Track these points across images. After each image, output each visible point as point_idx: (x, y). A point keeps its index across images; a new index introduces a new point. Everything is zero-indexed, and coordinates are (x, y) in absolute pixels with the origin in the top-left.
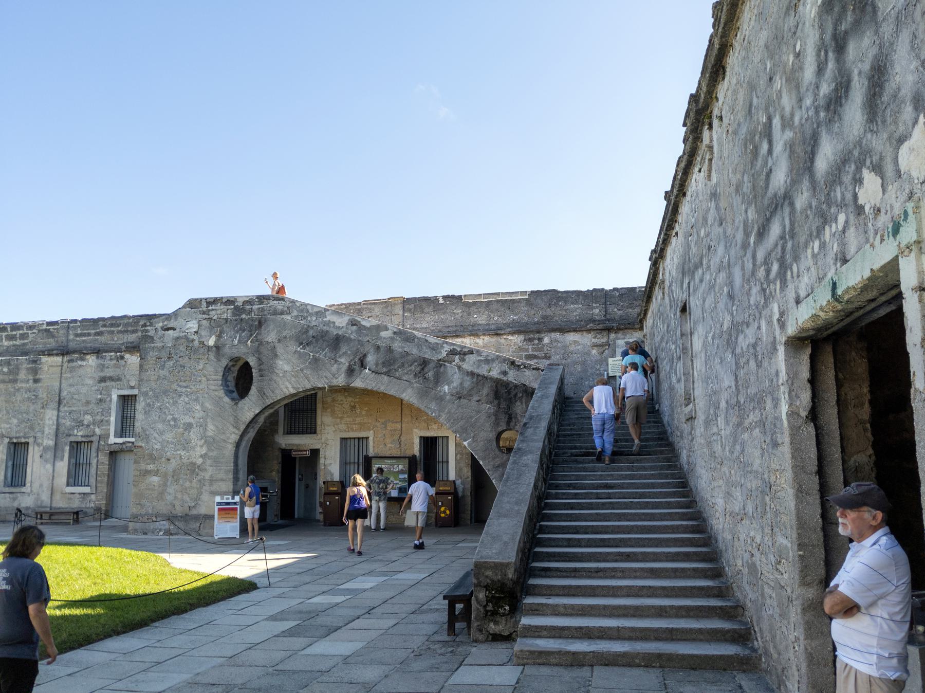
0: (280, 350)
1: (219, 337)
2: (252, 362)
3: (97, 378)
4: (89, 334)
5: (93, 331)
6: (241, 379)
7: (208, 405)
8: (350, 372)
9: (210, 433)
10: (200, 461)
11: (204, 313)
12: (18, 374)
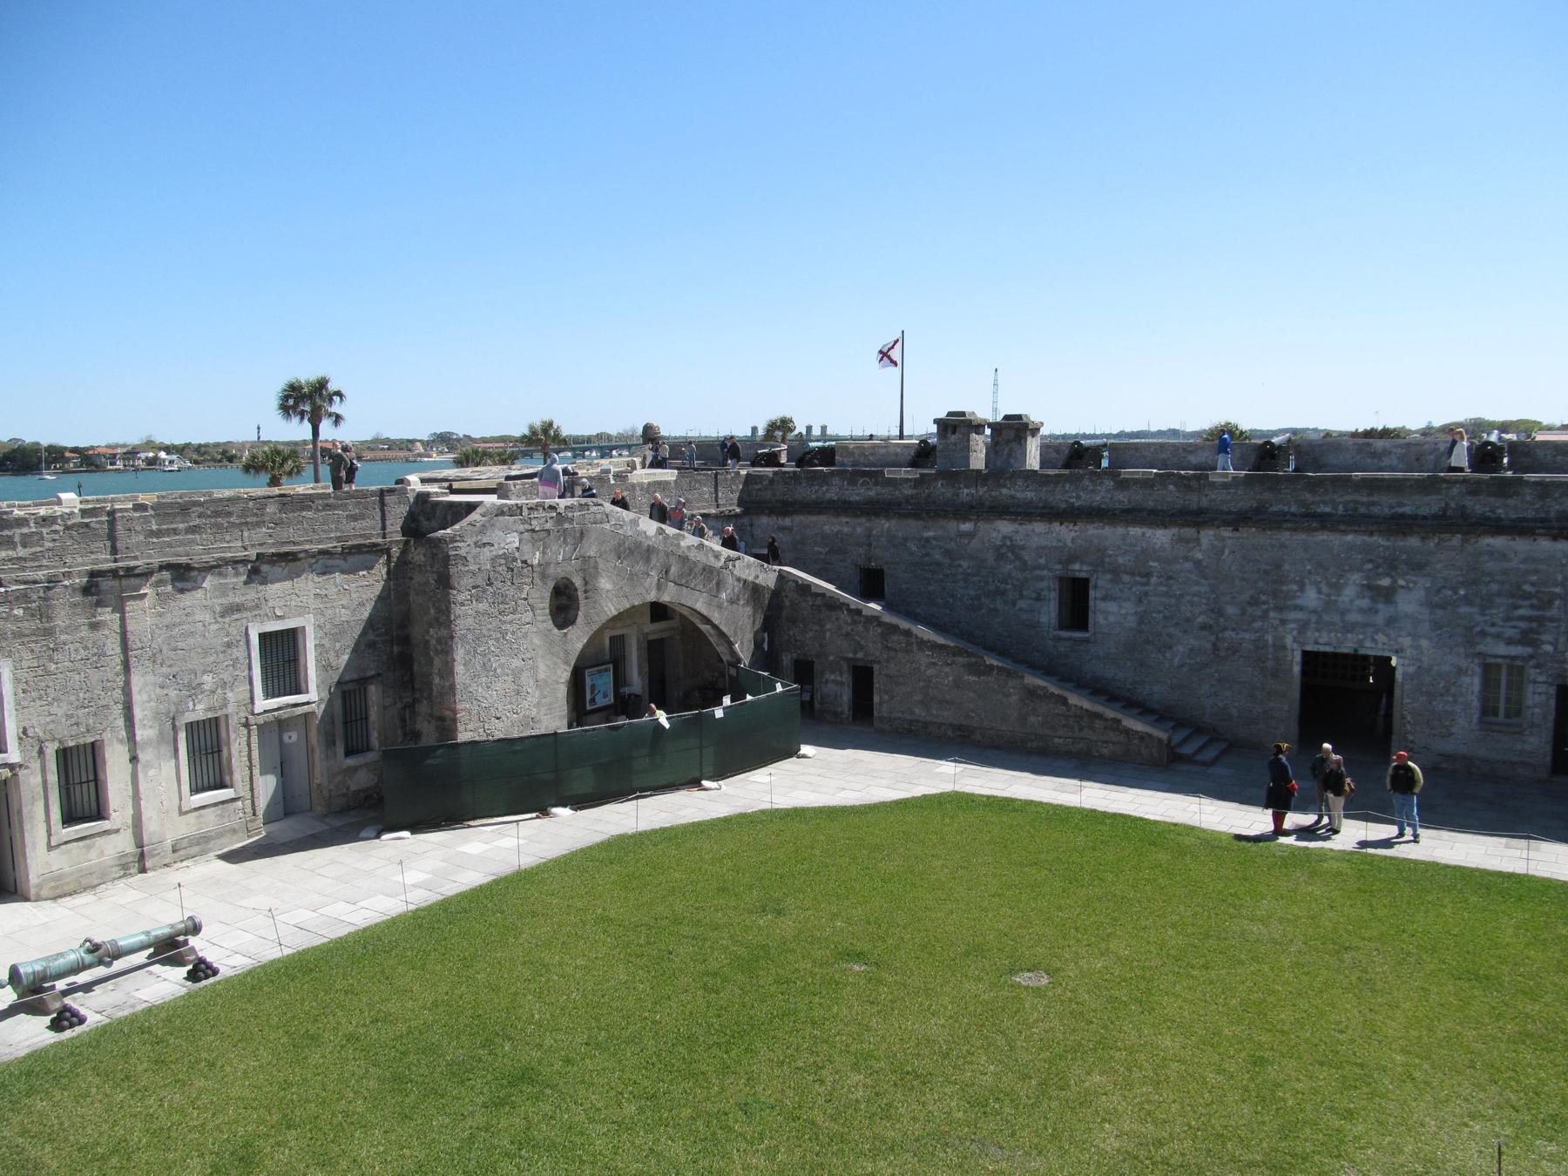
0: (601, 566)
1: (544, 553)
2: (578, 582)
3: (218, 609)
4: (175, 532)
5: (181, 526)
6: (564, 604)
7: (537, 641)
8: (659, 587)
9: (541, 676)
10: (534, 712)
11: (524, 522)
12: (50, 619)
